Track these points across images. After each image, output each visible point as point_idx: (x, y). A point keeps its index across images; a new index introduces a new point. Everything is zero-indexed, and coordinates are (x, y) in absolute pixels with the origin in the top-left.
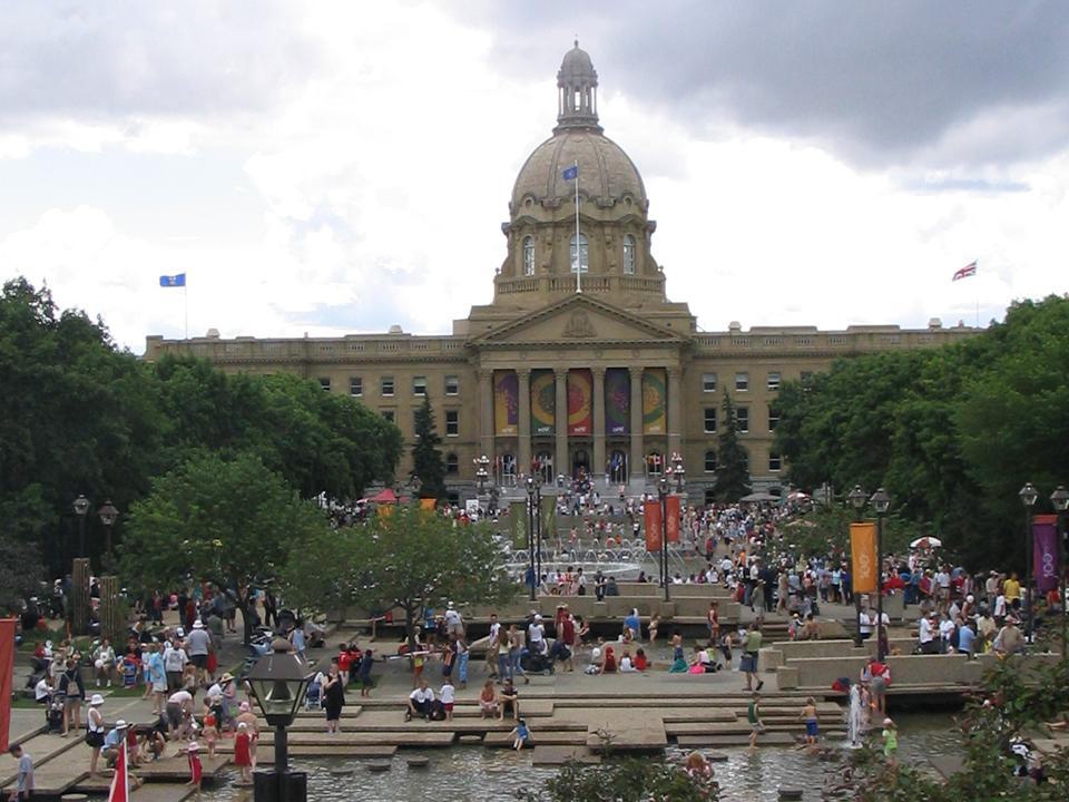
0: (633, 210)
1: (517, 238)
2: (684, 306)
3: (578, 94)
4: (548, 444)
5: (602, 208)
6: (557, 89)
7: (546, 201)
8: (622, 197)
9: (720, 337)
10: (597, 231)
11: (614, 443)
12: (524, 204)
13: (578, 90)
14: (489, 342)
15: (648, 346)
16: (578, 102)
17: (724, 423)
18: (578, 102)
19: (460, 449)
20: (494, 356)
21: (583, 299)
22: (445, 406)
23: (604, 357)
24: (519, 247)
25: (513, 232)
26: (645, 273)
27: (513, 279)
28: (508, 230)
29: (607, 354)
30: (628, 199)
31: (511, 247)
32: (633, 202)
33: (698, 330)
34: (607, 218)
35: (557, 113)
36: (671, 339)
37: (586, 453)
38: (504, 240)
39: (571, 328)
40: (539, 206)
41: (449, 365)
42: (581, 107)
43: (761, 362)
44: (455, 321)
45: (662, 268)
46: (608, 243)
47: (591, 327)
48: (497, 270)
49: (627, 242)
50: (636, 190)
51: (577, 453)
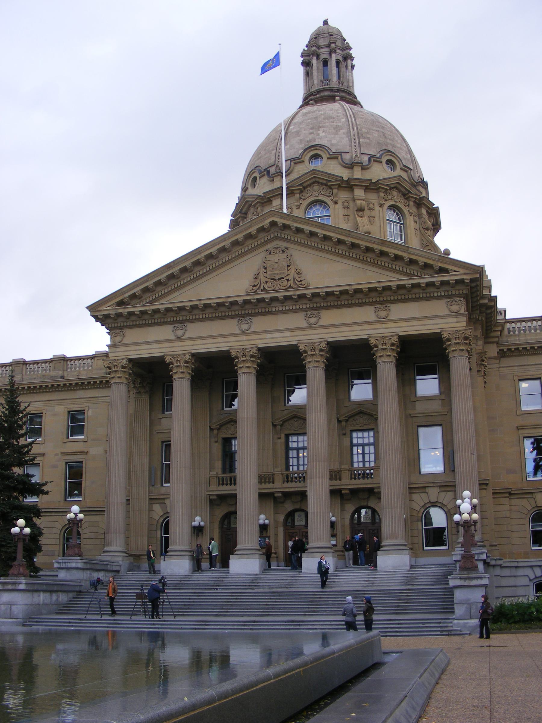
5: (350, 166)
10: (344, 195)
11: (354, 492)
23: (321, 323)
32: (398, 167)
34: (358, 174)
36: (445, 277)
39: (262, 277)
40: (265, 179)
46: (361, 210)
50: (402, 154)
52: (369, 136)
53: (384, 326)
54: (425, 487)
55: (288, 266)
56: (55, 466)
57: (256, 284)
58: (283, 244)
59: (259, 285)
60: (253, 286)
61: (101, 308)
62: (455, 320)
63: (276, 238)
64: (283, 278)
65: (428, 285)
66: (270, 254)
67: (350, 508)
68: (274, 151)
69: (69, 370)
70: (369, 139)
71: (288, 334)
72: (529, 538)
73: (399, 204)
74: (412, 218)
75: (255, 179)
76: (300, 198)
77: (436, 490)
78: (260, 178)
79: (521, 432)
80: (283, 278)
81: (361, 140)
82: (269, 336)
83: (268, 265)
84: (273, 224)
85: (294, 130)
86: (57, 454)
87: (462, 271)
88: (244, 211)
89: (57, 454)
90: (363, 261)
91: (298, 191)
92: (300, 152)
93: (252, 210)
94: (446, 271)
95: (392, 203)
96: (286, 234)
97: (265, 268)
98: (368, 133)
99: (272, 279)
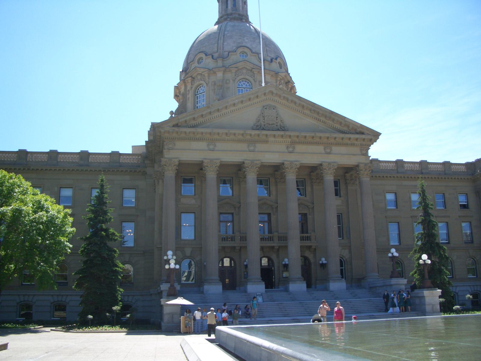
1: (189, 88)
7: (216, 55)
8: (276, 59)
20: (179, 144)
48: (172, 113)
55: (277, 118)
57: (258, 125)
59: (260, 126)
60: (256, 126)
64: (274, 124)
66: (266, 109)
68: (216, 45)
75: (201, 58)
76: (235, 75)
78: (206, 59)
80: (274, 124)
85: (228, 35)
91: (235, 71)
92: (234, 48)
93: (199, 77)
94: (363, 133)
97: (264, 117)
99: (267, 124)
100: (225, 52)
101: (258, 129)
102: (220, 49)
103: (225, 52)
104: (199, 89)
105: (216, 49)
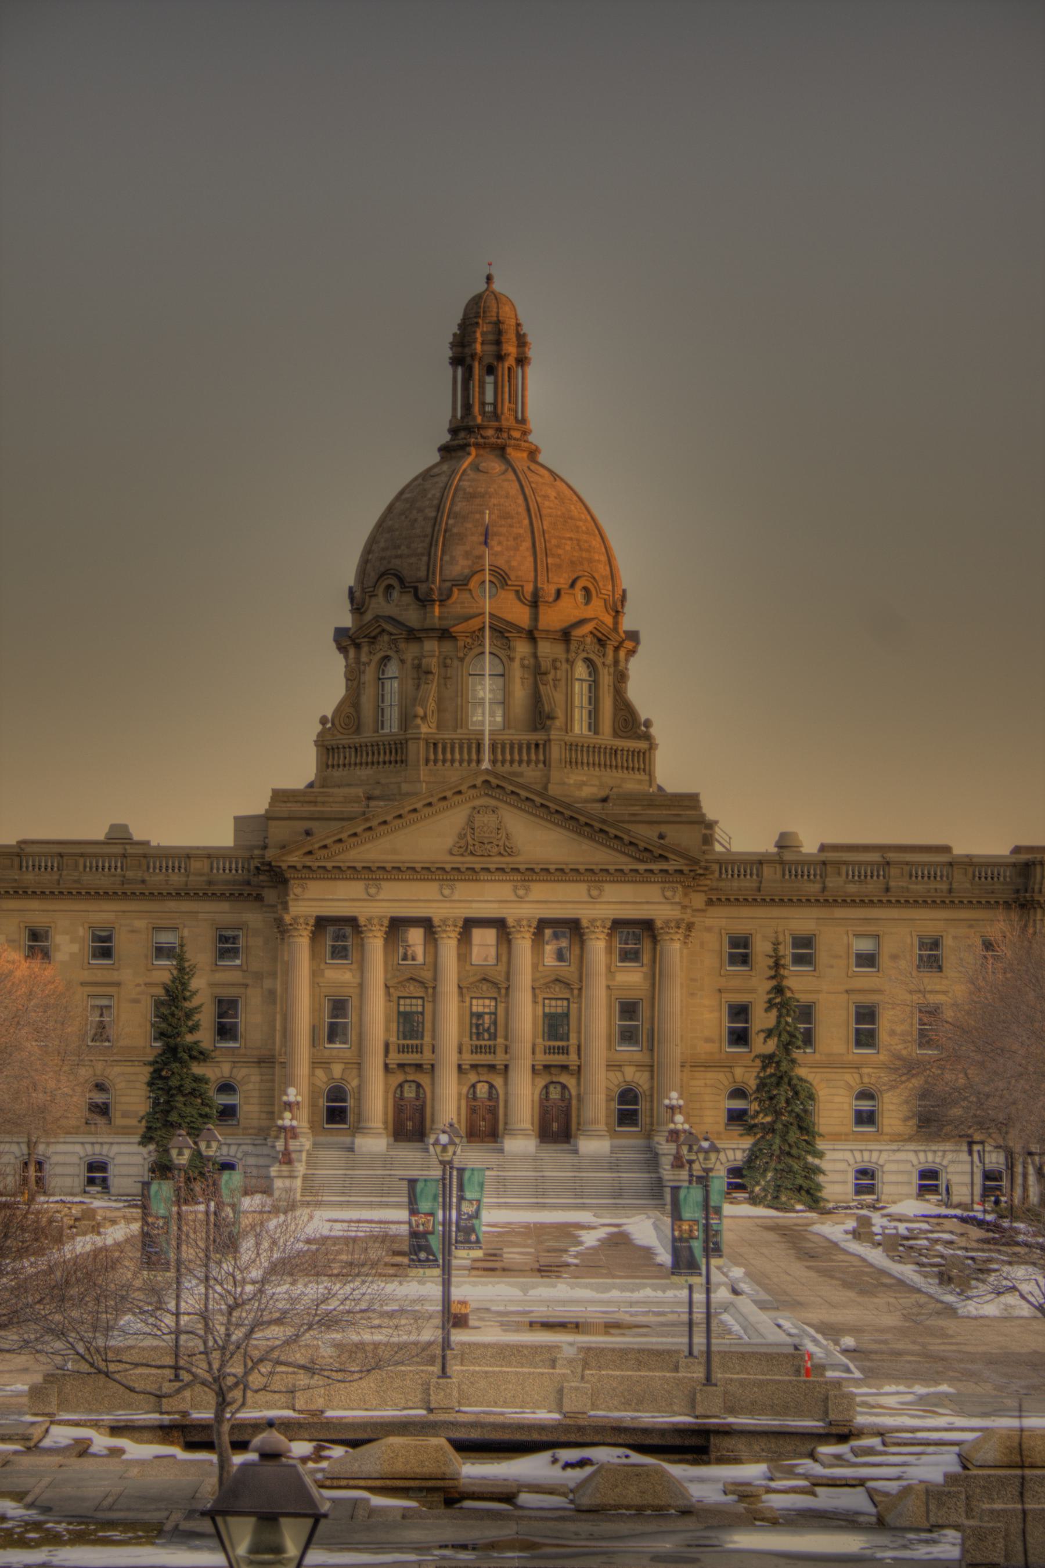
0: (596, 609)
1: (364, 659)
2: (691, 801)
3: (490, 379)
4: (419, 1067)
6: (449, 370)
7: (423, 588)
9: (760, 863)
11: (547, 1067)
12: (380, 591)
13: (490, 370)
14: (308, 861)
15: (620, 876)
16: (489, 397)
17: (769, 1033)
18: (489, 397)
19: (241, 1073)
20: (316, 889)
21: (494, 781)
22: (212, 985)
23: (531, 897)
24: (369, 675)
25: (358, 646)
26: (616, 734)
27: (356, 740)
28: (345, 640)
29: (539, 891)
30: (586, 589)
31: (353, 677)
33: (718, 848)
35: (449, 415)
36: (664, 866)
37: (491, 1086)
38: (338, 664)
40: (408, 599)
41: (225, 906)
42: (495, 405)
43: (840, 913)
44: (238, 820)
45: (648, 724)
47: (508, 837)
48: (323, 721)
49: (581, 670)
51: (474, 1086)
52: (560, 551)
53: (598, 906)
54: (620, 1066)
56: (136, 1001)
58: (493, 802)
61: (284, 858)
62: (668, 907)
63: (487, 795)
65: (646, 870)
67: (541, 1082)
68: (425, 559)
69: (151, 870)
70: (559, 556)
71: (495, 905)
72: (723, 1117)
73: (592, 656)
74: (606, 671)
75: (389, 587)
77: (632, 1069)
79: (724, 995)
81: (550, 560)
82: (474, 905)
83: (476, 826)
84: (486, 782)
86: (138, 985)
87: (682, 861)
88: (373, 634)
89: (138, 985)
90: (580, 834)
93: (386, 638)
94: (666, 859)
95: (584, 655)
96: (497, 793)
97: (473, 829)
98: (558, 546)
100: (445, 581)
101: (462, 855)
102: (434, 574)
103: (445, 581)
104: (385, 665)
105: (422, 574)
